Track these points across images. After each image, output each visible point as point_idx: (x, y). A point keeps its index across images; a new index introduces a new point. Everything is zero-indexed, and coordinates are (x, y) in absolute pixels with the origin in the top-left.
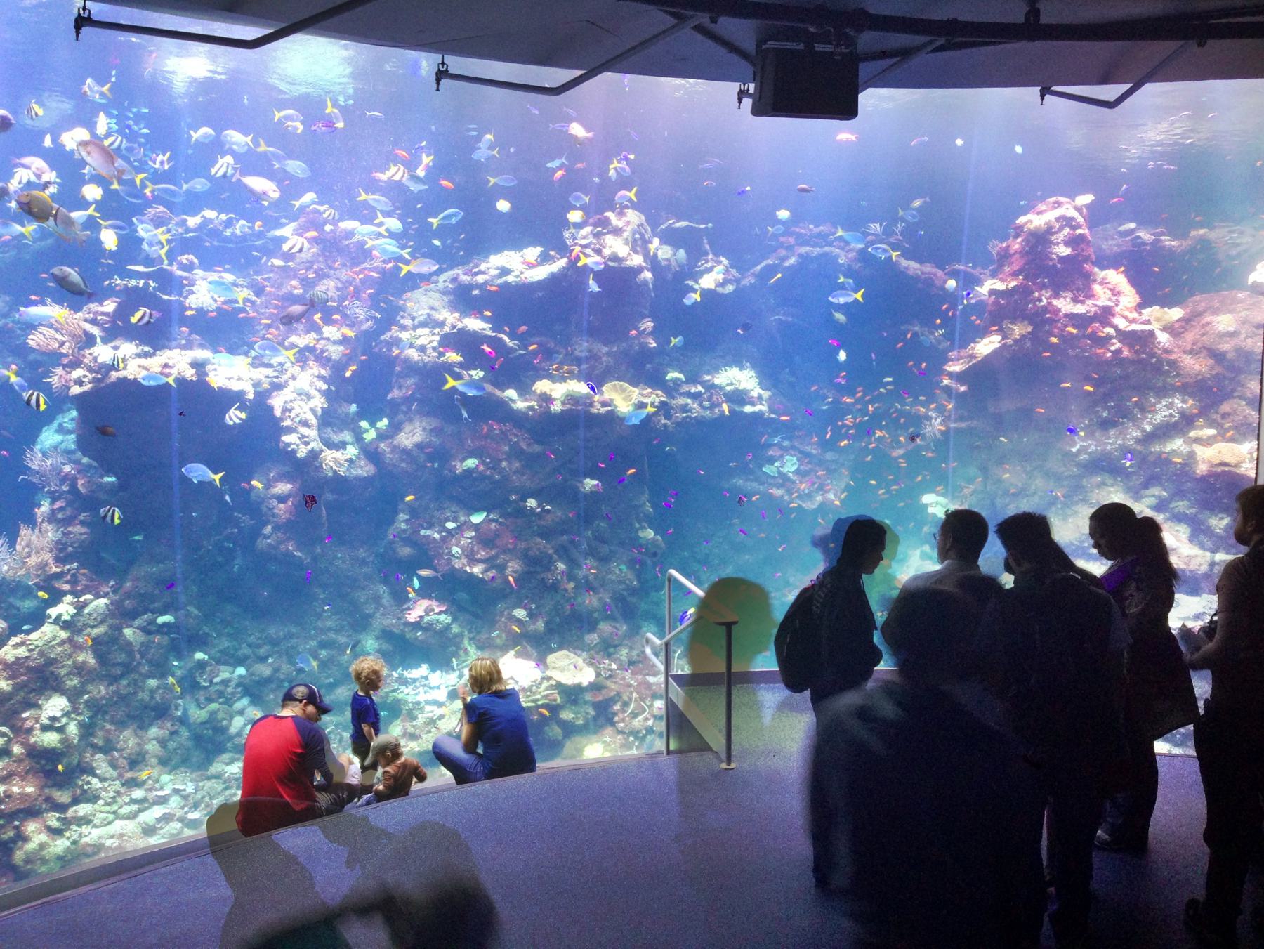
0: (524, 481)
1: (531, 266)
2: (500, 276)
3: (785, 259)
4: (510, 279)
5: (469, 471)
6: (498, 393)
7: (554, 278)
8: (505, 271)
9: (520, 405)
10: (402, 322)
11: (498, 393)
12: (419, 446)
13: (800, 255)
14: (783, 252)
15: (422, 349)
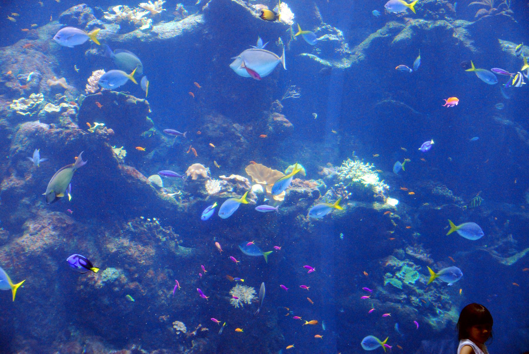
0: (165, 295)
1: (157, 19)
2: (121, 32)
3: (397, 31)
4: (138, 33)
5: (109, 285)
6: (141, 176)
7: (187, 37)
8: (127, 25)
9: (169, 194)
10: (9, 85)
11: (141, 176)
12: (49, 251)
13: (414, 28)
14: (392, 24)
15: (51, 118)
